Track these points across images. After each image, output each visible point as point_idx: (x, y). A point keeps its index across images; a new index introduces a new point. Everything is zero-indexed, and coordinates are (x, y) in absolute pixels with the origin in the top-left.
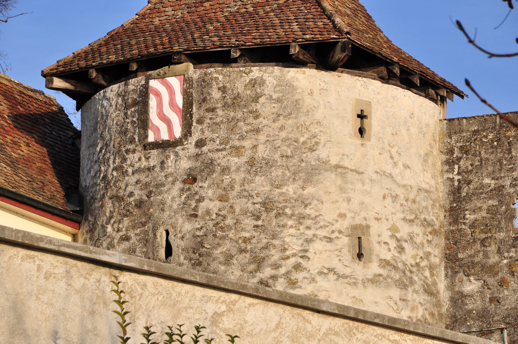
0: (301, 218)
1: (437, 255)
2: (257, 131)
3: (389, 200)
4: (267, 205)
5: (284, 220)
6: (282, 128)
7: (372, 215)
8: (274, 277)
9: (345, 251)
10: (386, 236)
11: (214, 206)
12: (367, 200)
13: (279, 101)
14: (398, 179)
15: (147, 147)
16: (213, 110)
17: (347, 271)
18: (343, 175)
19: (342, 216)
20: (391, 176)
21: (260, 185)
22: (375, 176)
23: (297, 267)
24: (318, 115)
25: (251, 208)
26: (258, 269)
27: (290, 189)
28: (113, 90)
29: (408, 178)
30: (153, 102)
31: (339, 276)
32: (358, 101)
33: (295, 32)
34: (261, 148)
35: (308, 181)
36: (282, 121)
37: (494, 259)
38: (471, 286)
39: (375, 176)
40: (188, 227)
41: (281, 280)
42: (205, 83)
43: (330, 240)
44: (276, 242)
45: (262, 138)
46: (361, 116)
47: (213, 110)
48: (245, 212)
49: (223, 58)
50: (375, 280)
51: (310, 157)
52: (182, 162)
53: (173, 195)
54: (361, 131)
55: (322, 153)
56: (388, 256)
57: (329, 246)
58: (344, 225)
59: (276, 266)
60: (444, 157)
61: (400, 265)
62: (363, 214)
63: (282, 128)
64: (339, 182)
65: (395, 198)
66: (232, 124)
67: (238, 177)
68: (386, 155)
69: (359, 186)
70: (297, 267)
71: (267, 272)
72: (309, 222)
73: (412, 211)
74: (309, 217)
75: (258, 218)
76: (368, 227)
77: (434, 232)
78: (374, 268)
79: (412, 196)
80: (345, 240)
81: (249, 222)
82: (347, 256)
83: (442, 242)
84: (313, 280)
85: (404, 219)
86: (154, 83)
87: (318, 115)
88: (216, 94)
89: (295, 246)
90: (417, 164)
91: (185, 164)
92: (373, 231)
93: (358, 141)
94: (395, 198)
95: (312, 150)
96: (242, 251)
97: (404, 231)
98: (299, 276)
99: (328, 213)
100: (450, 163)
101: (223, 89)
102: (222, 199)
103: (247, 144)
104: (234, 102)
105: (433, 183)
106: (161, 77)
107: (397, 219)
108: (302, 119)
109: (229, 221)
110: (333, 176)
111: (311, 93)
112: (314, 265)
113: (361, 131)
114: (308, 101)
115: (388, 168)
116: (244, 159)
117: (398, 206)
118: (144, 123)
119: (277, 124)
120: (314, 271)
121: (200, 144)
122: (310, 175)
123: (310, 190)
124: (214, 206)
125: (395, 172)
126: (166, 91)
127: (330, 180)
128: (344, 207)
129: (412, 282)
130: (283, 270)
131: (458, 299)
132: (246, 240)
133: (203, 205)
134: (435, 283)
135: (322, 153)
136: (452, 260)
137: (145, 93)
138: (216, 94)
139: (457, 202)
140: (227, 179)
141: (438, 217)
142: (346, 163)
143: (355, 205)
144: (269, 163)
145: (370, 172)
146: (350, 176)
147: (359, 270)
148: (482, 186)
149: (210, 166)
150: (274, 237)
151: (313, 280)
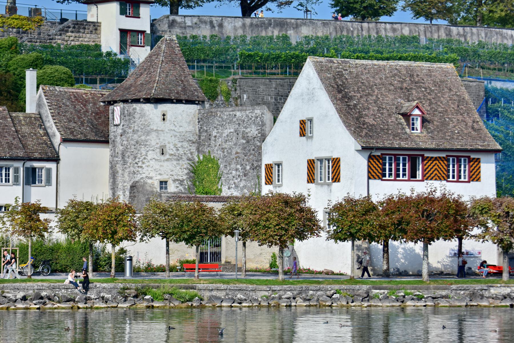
0: (146, 145)
1: (194, 149)
2: (135, 122)
3: (173, 137)
4: (137, 142)
5: (141, 146)
6: (141, 121)
7: (167, 142)
8: (139, 161)
9: (158, 153)
10: (172, 147)
11: (125, 142)
12: (165, 138)
13: (140, 113)
14: (178, 131)
15: (115, 125)
16: (125, 116)
17: (159, 158)
18: (158, 133)
19: (157, 143)
20: (174, 130)
21: (136, 137)
22: (168, 131)
23: (145, 158)
24: (151, 116)
25: (133, 143)
26: (135, 159)
27: (143, 138)
29: (181, 129)
30: (115, 113)
31: (156, 160)
32: (162, 111)
33: (143, 95)
34: (136, 127)
35: (147, 135)
36: (141, 119)
37: (205, 150)
39: (168, 131)
40: (121, 148)
41: (141, 163)
42: (124, 109)
43: (154, 150)
44: (139, 152)
45: (136, 124)
46: (164, 115)
47: (125, 116)
48: (132, 144)
50: (167, 160)
51: (148, 128)
52: (120, 131)
53: (118, 139)
54: (164, 119)
55: (151, 127)
56: (173, 153)
57: (153, 152)
58: (158, 146)
59: (139, 158)
60: (197, 120)
61: (177, 155)
62: (164, 142)
63: (141, 121)
64: (156, 134)
65: (175, 136)
67: (131, 135)
68: (173, 125)
69: (163, 135)
70: (145, 158)
71: (137, 160)
72: (148, 146)
73: (182, 139)
74: (148, 145)
75: (135, 146)
76: (166, 146)
77: (194, 143)
78: (168, 156)
79: (183, 134)
80: (158, 150)
81: (133, 147)
82: (159, 154)
83: (196, 145)
84: (149, 162)
85: (179, 142)
86: (115, 108)
87: (151, 116)
88: (126, 112)
89: (144, 153)
90: (185, 125)
91: (121, 131)
92: (168, 145)
93: (163, 122)
94: (175, 136)
95: (148, 126)
96: (132, 155)
97: (179, 145)
98: (145, 161)
99: (153, 143)
100: (199, 122)
101: (127, 111)
102: (127, 141)
103: (132, 126)
105: (193, 129)
106: (116, 106)
107: (176, 142)
108: (146, 118)
109: (129, 147)
110: (154, 133)
111: (148, 111)
112: (149, 158)
113: (164, 119)
114: (148, 113)
115: (173, 128)
116: (131, 130)
117: (177, 138)
118: (113, 119)
119: (139, 120)
120: (149, 159)
121: (123, 126)
122: (148, 133)
123: (148, 137)
124: (125, 142)
125: (176, 129)
127: (154, 135)
128: (158, 141)
129: (181, 158)
130: (141, 160)
132: (133, 152)
133: (124, 142)
134: (193, 157)
135: (151, 127)
137: (113, 110)
138: (126, 112)
140: (128, 135)
141: (194, 138)
142: (159, 129)
143: (161, 140)
144: (138, 131)
145: (167, 130)
146: (160, 132)
147: (163, 158)
148: (204, 129)
149: (125, 131)
150: (139, 151)
151: (149, 162)
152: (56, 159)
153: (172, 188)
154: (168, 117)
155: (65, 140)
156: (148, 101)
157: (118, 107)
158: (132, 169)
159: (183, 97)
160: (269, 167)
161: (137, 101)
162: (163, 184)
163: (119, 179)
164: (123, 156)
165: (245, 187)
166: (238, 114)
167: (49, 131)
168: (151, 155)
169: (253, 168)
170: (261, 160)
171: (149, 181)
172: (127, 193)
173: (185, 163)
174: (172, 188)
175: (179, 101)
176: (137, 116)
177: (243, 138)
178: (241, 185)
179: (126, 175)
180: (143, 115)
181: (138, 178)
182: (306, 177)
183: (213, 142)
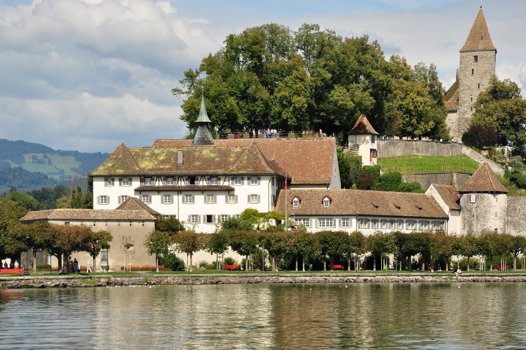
4: (485, 211)
21: (485, 209)
28: (466, 194)
33: (488, 189)
38: (509, 218)
42: (478, 196)
49: (480, 192)
52: (475, 205)
53: (474, 209)
66: (481, 201)
99: (493, 211)
122: (490, 207)
126: (473, 196)
127: (493, 207)
131: (508, 220)
136: (507, 215)
139: (508, 207)
141: (506, 209)
147: (496, 218)
149: (478, 206)
152: (448, 219)
154: (498, 200)
156: (492, 193)
157: (474, 195)
158: (482, 223)
159: (503, 191)
164: (477, 217)
167: (440, 205)
168: (492, 217)
171: (491, 229)
173: (503, 220)
175: (503, 193)
176: (485, 199)
179: (479, 226)
180: (488, 199)
183: (517, 211)
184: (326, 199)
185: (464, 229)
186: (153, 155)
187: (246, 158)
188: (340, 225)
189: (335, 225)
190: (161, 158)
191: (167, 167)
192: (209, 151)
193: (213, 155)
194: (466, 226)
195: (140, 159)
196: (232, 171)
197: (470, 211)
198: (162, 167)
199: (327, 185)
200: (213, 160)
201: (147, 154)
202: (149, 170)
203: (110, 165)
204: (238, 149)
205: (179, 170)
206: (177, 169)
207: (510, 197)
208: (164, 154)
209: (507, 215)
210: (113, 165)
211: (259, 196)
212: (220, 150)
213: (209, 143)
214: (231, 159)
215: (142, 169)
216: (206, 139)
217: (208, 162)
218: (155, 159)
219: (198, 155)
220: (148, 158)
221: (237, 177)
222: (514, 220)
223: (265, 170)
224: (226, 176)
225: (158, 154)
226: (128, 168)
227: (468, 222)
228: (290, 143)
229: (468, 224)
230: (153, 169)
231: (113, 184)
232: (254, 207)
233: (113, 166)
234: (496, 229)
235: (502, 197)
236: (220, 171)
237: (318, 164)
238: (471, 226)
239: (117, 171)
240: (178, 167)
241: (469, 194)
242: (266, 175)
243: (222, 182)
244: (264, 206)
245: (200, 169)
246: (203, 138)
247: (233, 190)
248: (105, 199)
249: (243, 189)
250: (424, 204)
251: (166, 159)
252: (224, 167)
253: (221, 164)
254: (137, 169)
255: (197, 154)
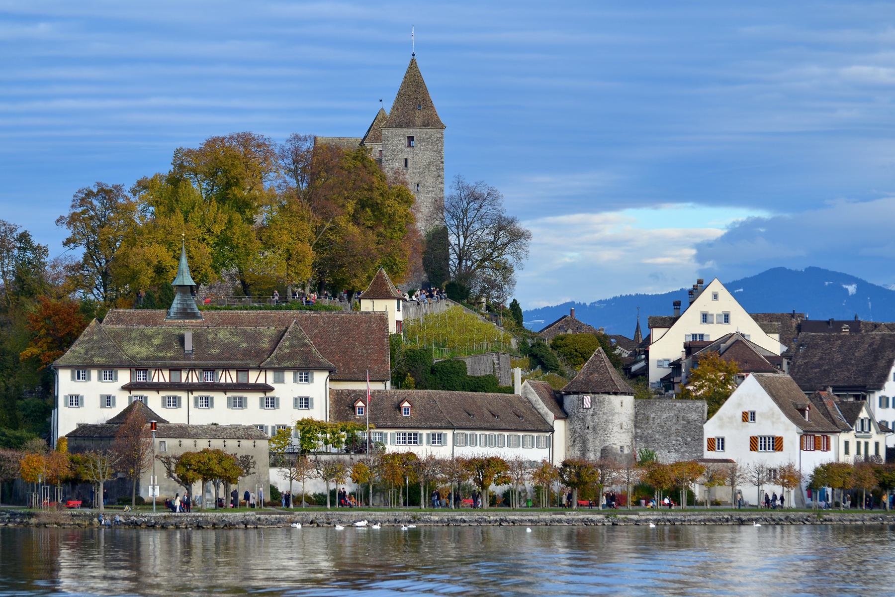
21: (605, 417)
28: (576, 396)
38: (639, 431)
52: (591, 412)
53: (589, 418)
104: (600, 402)
122: (613, 415)
126: (587, 399)
131: (636, 433)
136: (635, 426)
139: (636, 415)
141: (633, 418)
147: (622, 431)
152: (553, 431)
153: (626, 451)
155: (556, 418)
156: (616, 394)
160: (711, 441)
161: (609, 393)
162: (621, 447)
163: (590, 445)
164: (594, 428)
165: (685, 452)
166: (678, 404)
167: (541, 411)
169: (693, 439)
170: (703, 435)
172: (599, 454)
173: (630, 434)
174: (626, 451)
176: (606, 403)
177: (683, 420)
178: (682, 450)
180: (610, 403)
181: (607, 444)
182: (748, 447)
183: (651, 422)
184: (406, 404)
185: (573, 446)
186: (143, 337)
187: (287, 344)
188: (428, 442)
189: (421, 442)
190: (158, 341)
191: (169, 355)
192: (228, 333)
193: (235, 339)
194: (576, 442)
195: (125, 343)
196: (270, 362)
197: (583, 420)
198: (161, 355)
199: (383, 381)
200: (236, 346)
201: (133, 335)
202: (143, 359)
203: (82, 350)
204: (273, 331)
205: (189, 359)
206: (184, 359)
207: (639, 401)
208: (161, 336)
209: (636, 426)
210: (87, 352)
211: (312, 399)
212: (244, 332)
213: (194, 316)
214: (264, 345)
215: (133, 358)
216: (189, 311)
217: (229, 349)
218: (148, 344)
219: (214, 338)
220: (136, 342)
221: (279, 370)
222: (645, 433)
223: (320, 363)
224: (260, 369)
225: (151, 336)
226: (109, 356)
227: (580, 436)
228: (321, 318)
229: (577, 439)
230: (148, 358)
231: (89, 379)
232: (305, 414)
233: (87, 352)
234: (621, 447)
235: (629, 400)
236: (252, 363)
237: (367, 350)
238: (584, 442)
239: (95, 360)
240: (187, 356)
241: (581, 396)
242: (321, 369)
243: (184, 375)
244: (319, 412)
245: (221, 360)
246: (185, 309)
247: (272, 389)
248: (76, 401)
249: (288, 388)
250: (523, 410)
251: (165, 344)
252: (257, 357)
253: (250, 352)
254: (124, 357)
255: (210, 337)
